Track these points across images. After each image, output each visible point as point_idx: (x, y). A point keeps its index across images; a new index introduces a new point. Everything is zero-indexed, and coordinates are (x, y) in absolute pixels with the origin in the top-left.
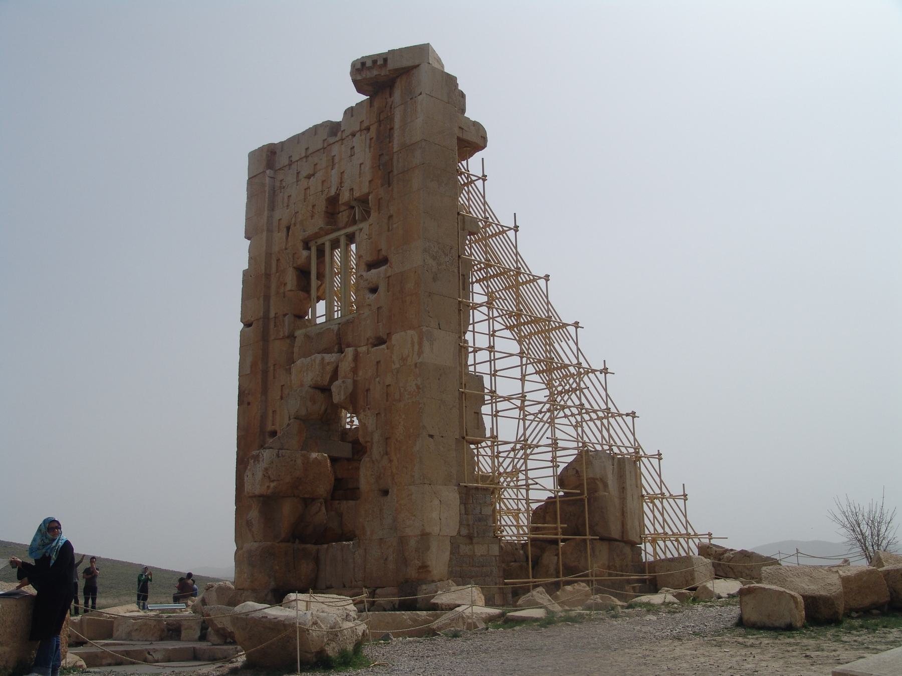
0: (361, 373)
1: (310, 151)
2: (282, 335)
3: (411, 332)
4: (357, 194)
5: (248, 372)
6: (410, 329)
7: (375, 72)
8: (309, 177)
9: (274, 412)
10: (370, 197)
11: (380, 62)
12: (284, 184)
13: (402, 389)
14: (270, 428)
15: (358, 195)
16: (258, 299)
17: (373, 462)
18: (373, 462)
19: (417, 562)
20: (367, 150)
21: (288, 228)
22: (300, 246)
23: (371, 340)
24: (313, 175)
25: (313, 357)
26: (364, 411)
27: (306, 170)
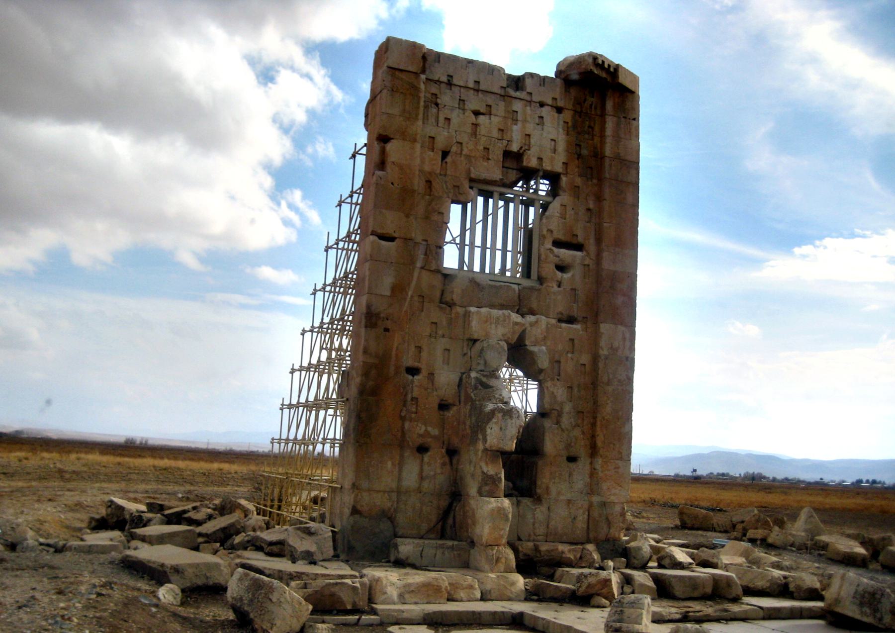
0: (549, 343)
1: (482, 87)
2: (433, 268)
3: (621, 328)
4: (547, 166)
5: (388, 293)
6: (621, 324)
7: (604, 75)
8: (477, 113)
9: (419, 349)
10: (564, 179)
11: (612, 70)
12: (439, 101)
13: (611, 376)
14: (410, 362)
15: (549, 168)
16: (407, 216)
17: (563, 430)
18: (563, 430)
19: (621, 525)
20: (561, 130)
21: (445, 154)
22: (466, 184)
23: (560, 316)
24: (483, 114)
25: (506, 312)
26: (552, 379)
27: (475, 102)
